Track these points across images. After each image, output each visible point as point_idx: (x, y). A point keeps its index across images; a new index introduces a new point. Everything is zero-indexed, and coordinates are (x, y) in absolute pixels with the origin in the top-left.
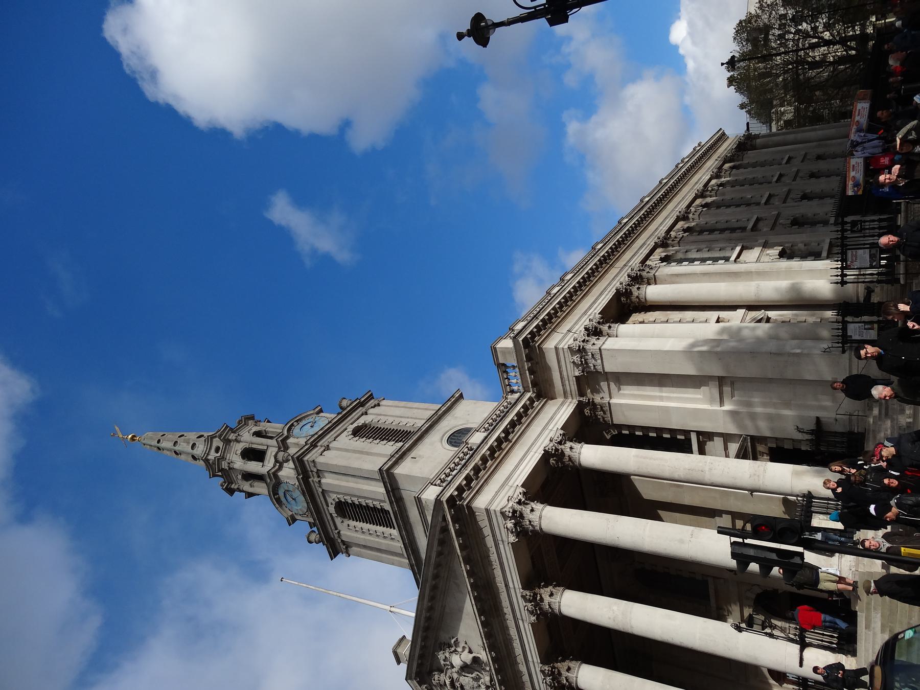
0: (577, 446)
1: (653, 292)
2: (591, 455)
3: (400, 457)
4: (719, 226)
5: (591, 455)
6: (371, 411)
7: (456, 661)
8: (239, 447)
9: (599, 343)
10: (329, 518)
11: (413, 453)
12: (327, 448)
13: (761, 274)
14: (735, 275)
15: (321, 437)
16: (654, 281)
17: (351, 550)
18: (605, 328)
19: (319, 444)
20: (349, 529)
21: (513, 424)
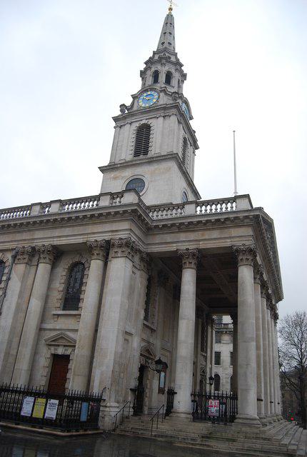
12: (179, 122)
17: (118, 129)
20: (130, 132)
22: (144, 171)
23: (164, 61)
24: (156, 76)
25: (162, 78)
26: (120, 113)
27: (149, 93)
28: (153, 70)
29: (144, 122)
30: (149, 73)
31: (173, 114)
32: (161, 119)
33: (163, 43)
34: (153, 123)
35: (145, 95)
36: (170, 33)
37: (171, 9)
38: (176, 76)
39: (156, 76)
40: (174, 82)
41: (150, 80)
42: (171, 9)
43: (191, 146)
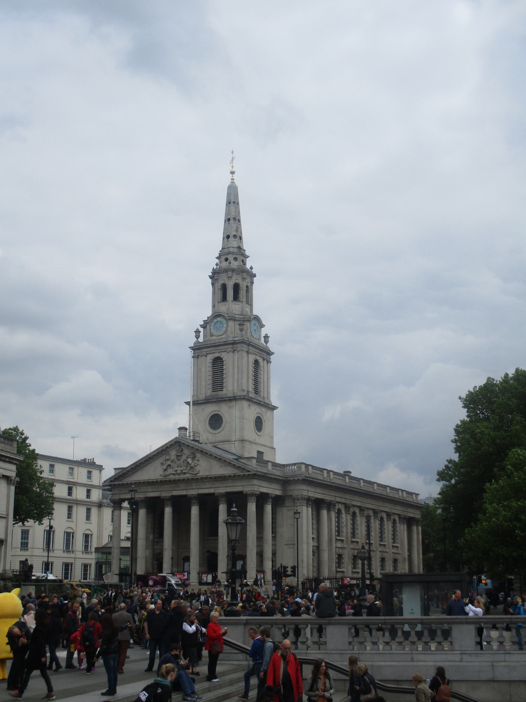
0: (270, 503)
1: (324, 513)
2: (268, 508)
3: (250, 400)
4: (356, 526)
5: (268, 508)
6: (265, 362)
7: (190, 460)
8: (239, 281)
9: (305, 504)
10: (213, 352)
11: (251, 404)
12: (248, 353)
13: (330, 550)
14: (330, 541)
15: (253, 346)
16: (329, 511)
18: (310, 503)
19: (250, 348)
21: (276, 479)
22: (223, 410)
23: (230, 274)
24: (224, 287)
25: (230, 293)
26: (196, 340)
27: (219, 319)
28: (221, 282)
29: (216, 355)
30: (219, 285)
31: (240, 350)
32: (231, 354)
33: (228, 237)
34: (224, 356)
35: (215, 321)
36: (234, 219)
37: (233, 173)
38: (243, 285)
39: (224, 287)
40: (242, 293)
41: (219, 294)
42: (233, 173)
43: (264, 359)
